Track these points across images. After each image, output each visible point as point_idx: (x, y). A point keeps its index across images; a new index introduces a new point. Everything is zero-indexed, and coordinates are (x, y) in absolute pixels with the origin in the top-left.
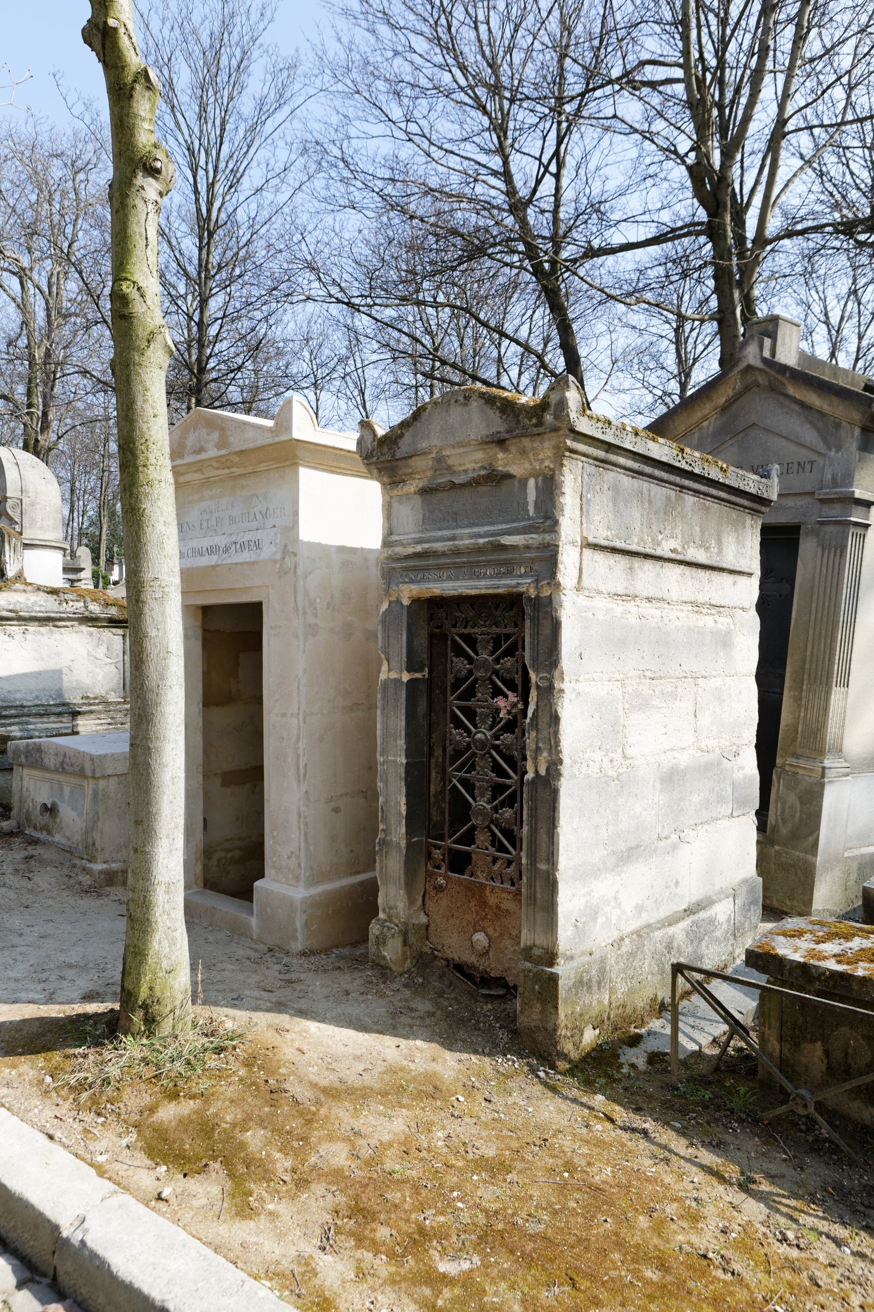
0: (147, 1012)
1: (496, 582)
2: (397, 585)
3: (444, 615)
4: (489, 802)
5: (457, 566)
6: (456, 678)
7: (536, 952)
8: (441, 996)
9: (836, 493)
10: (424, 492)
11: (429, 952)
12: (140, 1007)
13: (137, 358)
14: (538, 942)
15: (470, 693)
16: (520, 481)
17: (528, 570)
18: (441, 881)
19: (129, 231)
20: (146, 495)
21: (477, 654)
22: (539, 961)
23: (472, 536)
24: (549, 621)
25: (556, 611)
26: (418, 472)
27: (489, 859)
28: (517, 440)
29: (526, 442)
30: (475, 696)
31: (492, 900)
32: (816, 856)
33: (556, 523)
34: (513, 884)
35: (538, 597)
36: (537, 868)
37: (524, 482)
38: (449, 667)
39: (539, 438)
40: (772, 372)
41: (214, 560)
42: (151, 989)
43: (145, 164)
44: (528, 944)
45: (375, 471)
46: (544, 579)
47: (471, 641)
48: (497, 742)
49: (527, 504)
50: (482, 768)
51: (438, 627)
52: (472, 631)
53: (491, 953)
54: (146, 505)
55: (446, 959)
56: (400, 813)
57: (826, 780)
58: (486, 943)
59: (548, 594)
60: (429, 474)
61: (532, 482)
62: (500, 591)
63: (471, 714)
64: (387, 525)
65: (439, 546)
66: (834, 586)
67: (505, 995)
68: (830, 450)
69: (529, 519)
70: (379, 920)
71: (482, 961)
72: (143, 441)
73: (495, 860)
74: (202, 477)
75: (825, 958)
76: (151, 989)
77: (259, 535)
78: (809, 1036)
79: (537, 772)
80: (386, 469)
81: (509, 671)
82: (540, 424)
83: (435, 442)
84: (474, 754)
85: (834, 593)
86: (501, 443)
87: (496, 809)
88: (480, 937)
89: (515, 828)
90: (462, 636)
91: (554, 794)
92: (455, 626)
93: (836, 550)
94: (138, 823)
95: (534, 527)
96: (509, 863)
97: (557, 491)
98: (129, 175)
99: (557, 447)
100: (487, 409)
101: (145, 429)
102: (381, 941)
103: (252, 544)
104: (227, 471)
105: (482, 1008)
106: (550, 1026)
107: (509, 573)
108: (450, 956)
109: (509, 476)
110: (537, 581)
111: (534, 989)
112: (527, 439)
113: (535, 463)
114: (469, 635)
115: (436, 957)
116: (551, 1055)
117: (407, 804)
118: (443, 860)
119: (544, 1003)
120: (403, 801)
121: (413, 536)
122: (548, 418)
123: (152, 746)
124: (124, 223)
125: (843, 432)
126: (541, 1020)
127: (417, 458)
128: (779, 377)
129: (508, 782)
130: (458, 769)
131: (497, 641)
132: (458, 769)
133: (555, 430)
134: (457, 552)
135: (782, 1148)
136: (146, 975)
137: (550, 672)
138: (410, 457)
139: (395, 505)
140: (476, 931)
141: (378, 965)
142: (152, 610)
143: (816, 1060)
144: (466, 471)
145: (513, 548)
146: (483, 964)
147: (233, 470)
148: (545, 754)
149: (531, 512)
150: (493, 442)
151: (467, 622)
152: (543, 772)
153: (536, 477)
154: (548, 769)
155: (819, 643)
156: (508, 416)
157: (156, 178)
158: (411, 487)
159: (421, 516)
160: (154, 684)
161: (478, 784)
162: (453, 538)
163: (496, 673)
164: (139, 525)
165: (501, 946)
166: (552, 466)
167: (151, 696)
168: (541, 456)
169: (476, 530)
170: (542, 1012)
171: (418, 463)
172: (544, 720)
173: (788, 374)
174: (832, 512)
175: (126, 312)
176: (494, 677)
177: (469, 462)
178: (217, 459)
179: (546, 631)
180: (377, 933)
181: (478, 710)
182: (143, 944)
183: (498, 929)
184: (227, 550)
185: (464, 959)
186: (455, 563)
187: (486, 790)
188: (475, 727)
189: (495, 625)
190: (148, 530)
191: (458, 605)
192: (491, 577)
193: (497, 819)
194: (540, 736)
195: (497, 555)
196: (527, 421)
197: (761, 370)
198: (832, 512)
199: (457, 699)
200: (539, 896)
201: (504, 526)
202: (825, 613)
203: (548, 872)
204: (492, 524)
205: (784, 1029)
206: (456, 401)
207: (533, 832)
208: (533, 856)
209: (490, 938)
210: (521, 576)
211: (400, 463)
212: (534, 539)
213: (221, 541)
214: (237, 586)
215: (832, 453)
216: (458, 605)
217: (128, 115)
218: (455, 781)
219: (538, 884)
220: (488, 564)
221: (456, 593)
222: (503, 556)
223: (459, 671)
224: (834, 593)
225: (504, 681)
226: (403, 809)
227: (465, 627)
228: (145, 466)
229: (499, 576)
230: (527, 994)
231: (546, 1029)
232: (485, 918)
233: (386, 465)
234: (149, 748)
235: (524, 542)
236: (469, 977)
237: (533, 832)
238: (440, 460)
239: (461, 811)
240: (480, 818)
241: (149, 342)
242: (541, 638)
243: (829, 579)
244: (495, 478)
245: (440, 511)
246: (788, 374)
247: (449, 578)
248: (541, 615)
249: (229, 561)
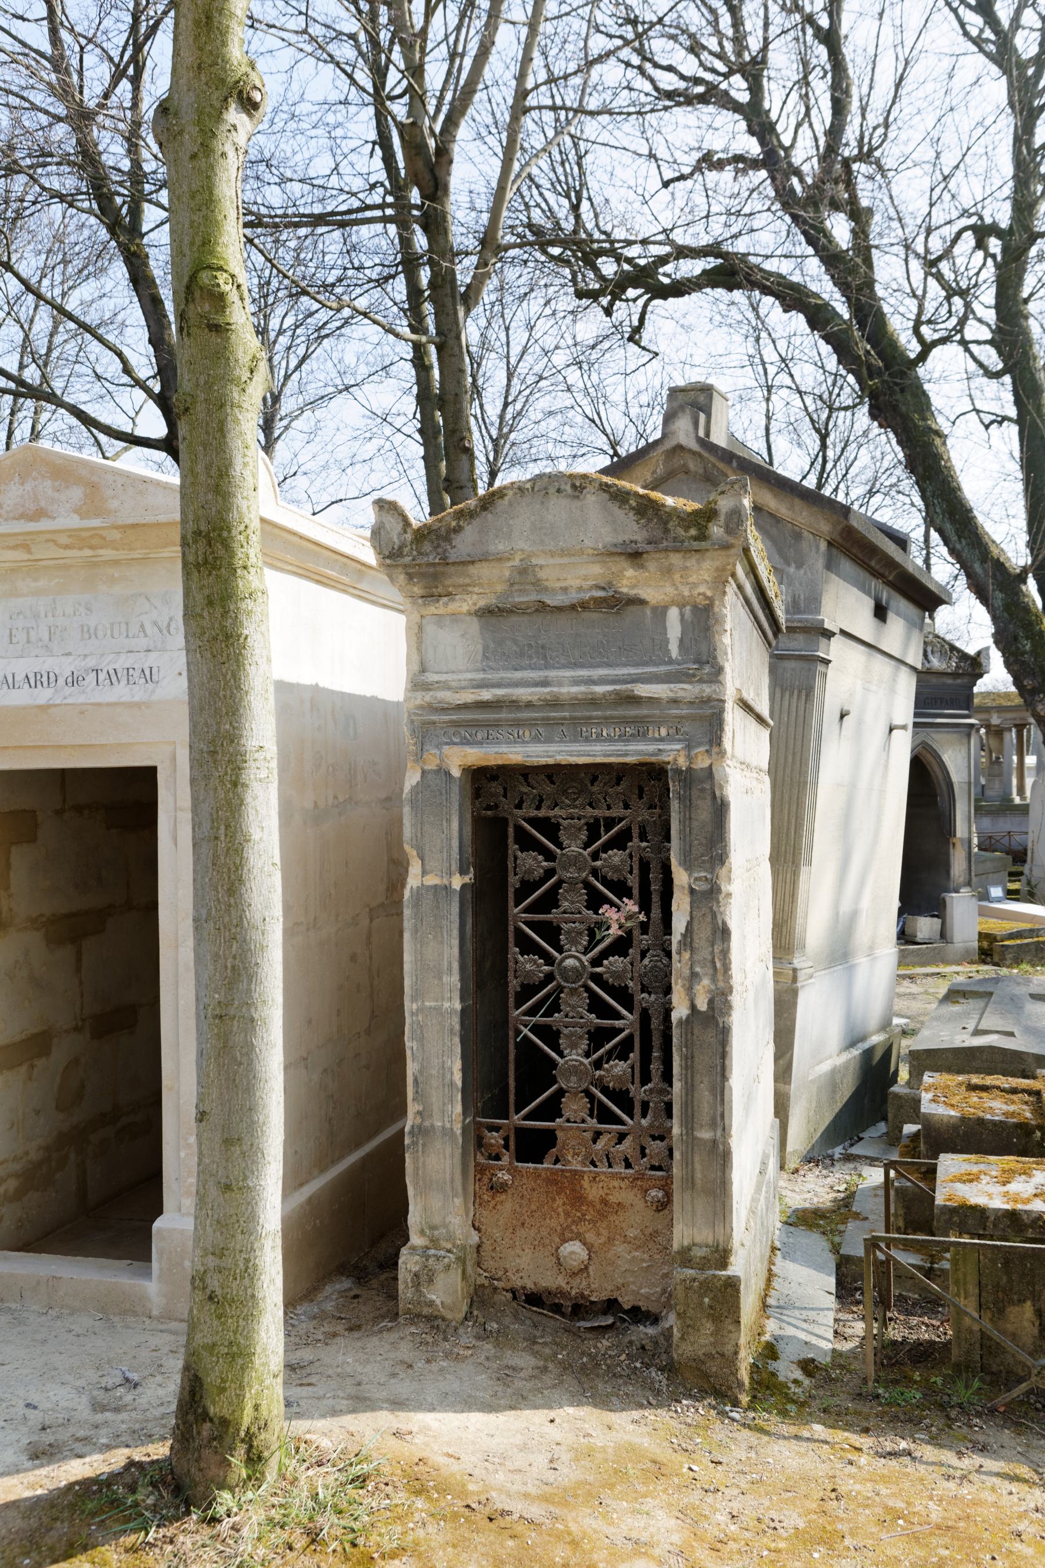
0: (251, 1446)
1: (620, 747)
2: (438, 746)
3: (500, 790)
4: (587, 1055)
5: (547, 722)
6: (523, 882)
7: (698, 1253)
8: (535, 1343)
9: (800, 621)
10: (488, 614)
11: (486, 1283)
12: (243, 1441)
13: (235, 395)
14: (698, 1239)
15: (550, 901)
16: (655, 609)
17: (672, 731)
18: (504, 1176)
19: (216, 192)
20: (249, 613)
21: (560, 846)
22: (704, 1264)
23: (576, 682)
24: (709, 801)
25: (721, 788)
26: (481, 585)
27: (588, 1135)
28: (663, 555)
29: (676, 559)
30: (557, 907)
31: (593, 1192)
32: (789, 1083)
33: (720, 670)
34: (628, 1165)
35: (689, 769)
36: (694, 1138)
37: (660, 612)
38: (510, 865)
39: (698, 556)
40: (712, 459)
41: (43, 695)
42: (256, 1408)
43: (241, 92)
44: (686, 1243)
45: (402, 577)
46: (700, 744)
47: (550, 828)
48: (599, 970)
49: (667, 641)
50: (573, 1007)
51: (488, 808)
52: (551, 813)
53: (591, 1269)
54: (249, 629)
55: (513, 1291)
56: (452, 1084)
57: (799, 985)
58: (584, 1254)
59: (706, 764)
60: (500, 588)
61: (673, 613)
62: (628, 760)
63: (551, 933)
64: (416, 657)
65: (523, 693)
66: (799, 737)
67: (613, 1324)
68: (789, 565)
69: (671, 662)
70: (413, 1248)
71: (575, 1282)
72: (242, 528)
73: (597, 1135)
74: (26, 557)
75: (1028, 1201)
76: (256, 1408)
77: (152, 660)
78: (1015, 1297)
79: (693, 1007)
80: (423, 575)
81: (616, 869)
82: (702, 536)
83: (521, 544)
84: (560, 989)
85: (799, 746)
86: (635, 556)
87: (598, 1065)
88: (574, 1250)
89: (632, 1088)
90: (533, 821)
91: (724, 1033)
92: (519, 806)
93: (800, 692)
94: (228, 1142)
95: (687, 675)
96: (621, 1137)
97: (717, 628)
98: (217, 104)
99: (721, 570)
100: (614, 507)
101: (244, 510)
102: (423, 1278)
103: (137, 674)
104: (88, 552)
105: (595, 1347)
106: (729, 1349)
107: (641, 735)
108: (519, 1283)
109: (642, 602)
110: (689, 747)
111: (701, 1303)
112: (679, 556)
113: (681, 587)
114: (547, 819)
115: (496, 1288)
116: (730, 1388)
117: (464, 1070)
118: (506, 1147)
119: (717, 1319)
120: (458, 1065)
121: (469, 676)
122: (716, 530)
123: (256, 1016)
124: (208, 177)
125: (804, 545)
126: (714, 1344)
127: (485, 564)
128: (721, 465)
129: (618, 1023)
130: (532, 1012)
131: (593, 830)
132: (532, 1012)
133: (726, 547)
134: (554, 703)
135: (1038, 1433)
136: (251, 1387)
137: (712, 870)
138: (473, 562)
139: (430, 629)
140: (565, 1241)
141: (419, 1316)
142: (255, 798)
143: (1026, 1324)
144: (565, 590)
145: (651, 701)
146: (576, 1287)
147: (101, 552)
148: (706, 982)
150: (621, 554)
151: (541, 801)
152: (702, 1005)
153: (681, 606)
154: (711, 1002)
155: (782, 811)
156: (650, 520)
157: (250, 115)
158: (464, 604)
159: (480, 647)
160: (258, 917)
161: (566, 1031)
162: (545, 683)
163: (595, 872)
164: (237, 661)
165: (610, 1255)
166: (709, 593)
167: (255, 936)
168: (693, 579)
169: (584, 673)
170: (716, 1333)
171: (483, 571)
172: (702, 934)
173: (735, 464)
174: (793, 644)
175: (221, 321)
176: (592, 879)
177: (573, 577)
178: (72, 532)
179: (703, 813)
180: (415, 1269)
181: (564, 926)
182: (247, 1338)
183: (605, 1233)
184: (74, 680)
185: (544, 1284)
186: (548, 719)
187: (581, 1037)
188: (560, 950)
189: (591, 805)
190: (251, 670)
191: (525, 776)
192: (610, 740)
193: (601, 1078)
194: (696, 957)
195: (626, 710)
196: (681, 531)
197: (694, 453)
198: (793, 644)
199: (526, 911)
200: (698, 1175)
201: (633, 671)
202: (788, 771)
203: (714, 1142)
204: (609, 665)
205: (984, 1294)
206: (559, 491)
207: (690, 1089)
208: (689, 1123)
209: (589, 1247)
210: (661, 740)
211: (452, 569)
212: (687, 690)
213: (65, 667)
214: (93, 742)
215: (792, 570)
216: (525, 776)
217: (221, 11)
218: (526, 1031)
219: (697, 1159)
220: (607, 721)
221: (551, 761)
222: (633, 712)
223: (530, 871)
224: (799, 746)
225: (605, 882)
226: (458, 1078)
227: (538, 808)
228: (245, 568)
229: (623, 738)
230: (690, 1313)
231: (723, 1355)
232: (582, 1219)
233: (424, 570)
234: (252, 1020)
235: (671, 695)
236: (557, 1309)
237: (690, 1089)
239: (536, 1071)
240: (574, 1079)
241: (252, 372)
242: (695, 824)
243: (792, 729)
244: (616, 603)
245: (515, 642)
246: (735, 464)
247: (536, 739)
248: (695, 793)
249: (82, 699)
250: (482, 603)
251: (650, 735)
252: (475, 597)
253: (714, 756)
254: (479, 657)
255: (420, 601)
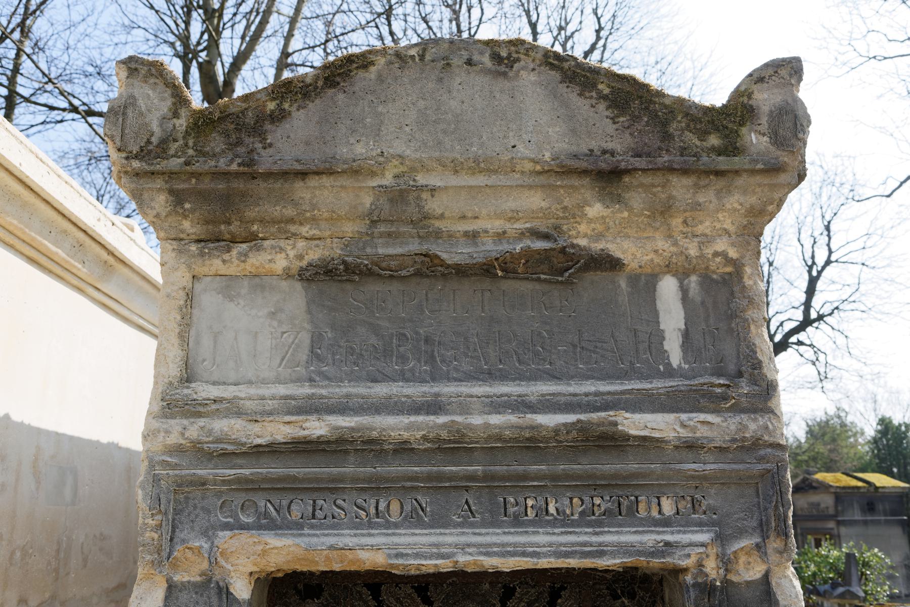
1: (584, 537)
5: (438, 485)
10: (321, 276)
16: (634, 279)
23: (497, 405)
26: (314, 220)
28: (658, 179)
37: (645, 285)
39: (721, 183)
46: (741, 533)
59: (755, 572)
60: (350, 229)
61: (668, 287)
65: (393, 426)
69: (670, 372)
80: (202, 196)
82: (732, 148)
83: (399, 147)
86: (608, 176)
100: (572, 95)
107: (623, 513)
109: (611, 264)
110: (721, 539)
112: (687, 181)
113: (683, 242)
121: (282, 390)
127: (326, 181)
134: (453, 446)
138: (303, 175)
139: (209, 301)
144: (473, 236)
145: (647, 444)
149: (676, 357)
150: (585, 172)
153: (682, 275)
156: (635, 118)
158: (278, 257)
159: (305, 338)
162: (434, 407)
166: (733, 253)
171: (322, 194)
177: (489, 214)
186: (440, 477)
192: (563, 521)
201: (604, 387)
204: (554, 377)
210: (666, 522)
211: (261, 187)
220: (556, 483)
221: (445, 566)
222: (609, 466)
229: (587, 519)
233: (207, 184)
235: (684, 433)
238: (401, 196)
244: (562, 266)
245: (375, 330)
247: (413, 519)
250: (314, 255)
251: (643, 513)
252: (301, 244)
253: (773, 557)
254: (303, 356)
255: (193, 248)
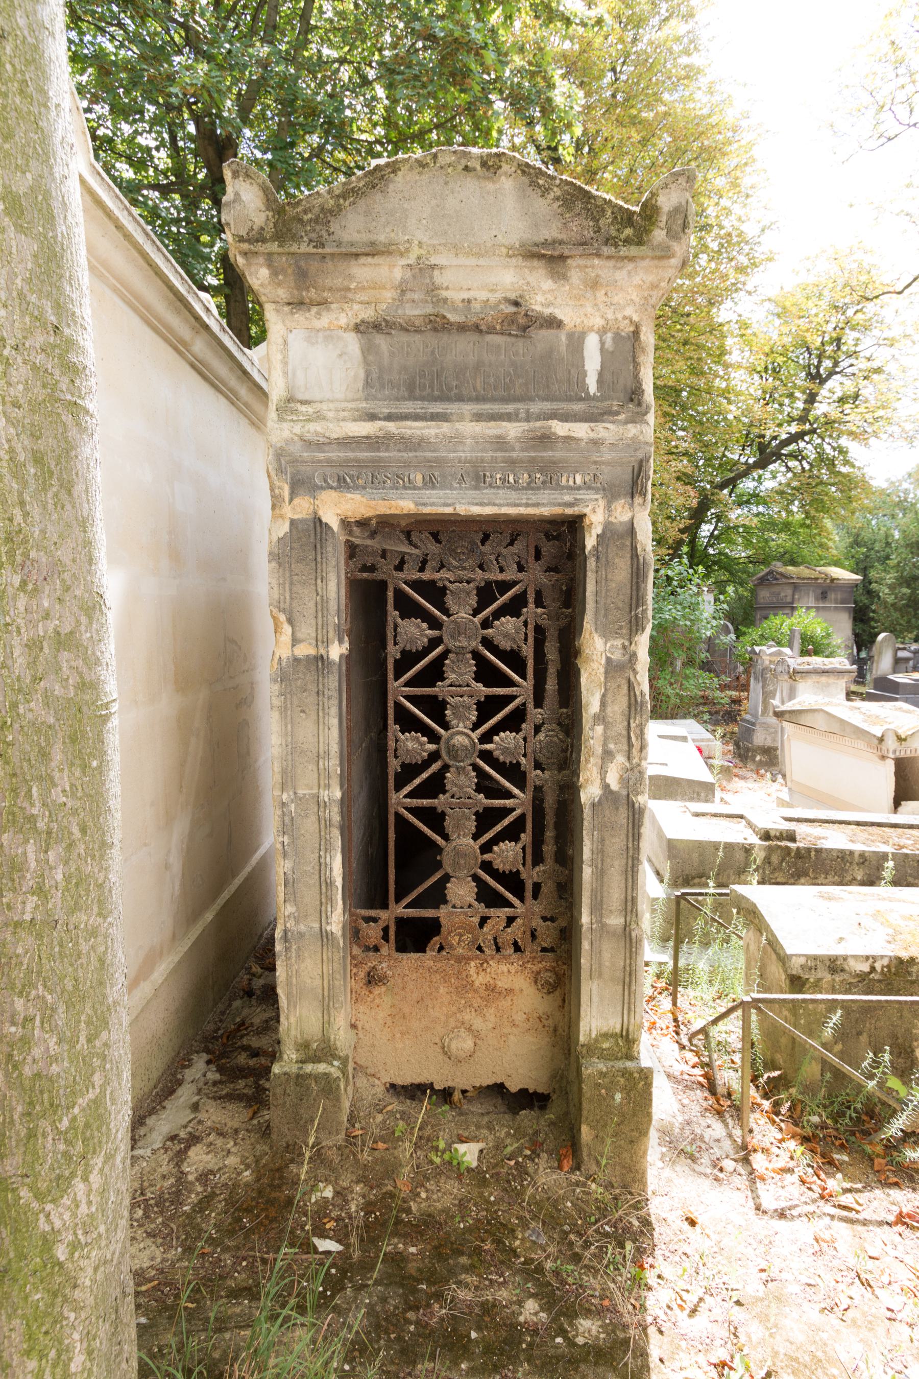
15: (435, 673)
16: (570, 336)
27: (476, 920)
38: (390, 634)
39: (630, 266)
47: (435, 592)
48: (489, 747)
52: (437, 576)
69: (588, 398)
73: (484, 920)
83: (420, 235)
84: (446, 768)
90: (417, 585)
96: (510, 920)
114: (433, 582)
129: (508, 803)
131: (486, 594)
138: (357, 255)
149: (593, 388)
150: (542, 257)
158: (342, 316)
159: (362, 374)
166: (636, 318)
189: (481, 567)
223: (412, 641)
227: (422, 569)
251: (564, 482)
252: (356, 307)
253: (637, 508)
254: (360, 385)
255: (287, 309)
